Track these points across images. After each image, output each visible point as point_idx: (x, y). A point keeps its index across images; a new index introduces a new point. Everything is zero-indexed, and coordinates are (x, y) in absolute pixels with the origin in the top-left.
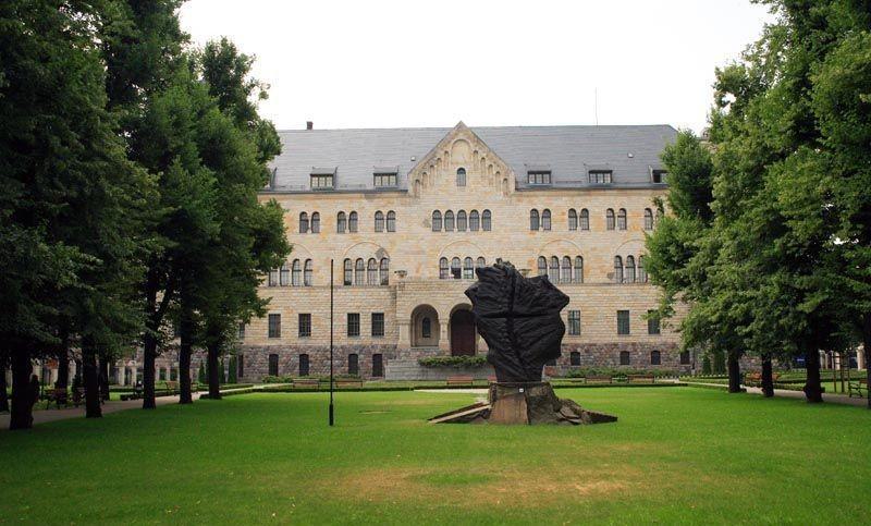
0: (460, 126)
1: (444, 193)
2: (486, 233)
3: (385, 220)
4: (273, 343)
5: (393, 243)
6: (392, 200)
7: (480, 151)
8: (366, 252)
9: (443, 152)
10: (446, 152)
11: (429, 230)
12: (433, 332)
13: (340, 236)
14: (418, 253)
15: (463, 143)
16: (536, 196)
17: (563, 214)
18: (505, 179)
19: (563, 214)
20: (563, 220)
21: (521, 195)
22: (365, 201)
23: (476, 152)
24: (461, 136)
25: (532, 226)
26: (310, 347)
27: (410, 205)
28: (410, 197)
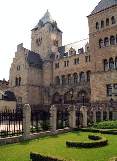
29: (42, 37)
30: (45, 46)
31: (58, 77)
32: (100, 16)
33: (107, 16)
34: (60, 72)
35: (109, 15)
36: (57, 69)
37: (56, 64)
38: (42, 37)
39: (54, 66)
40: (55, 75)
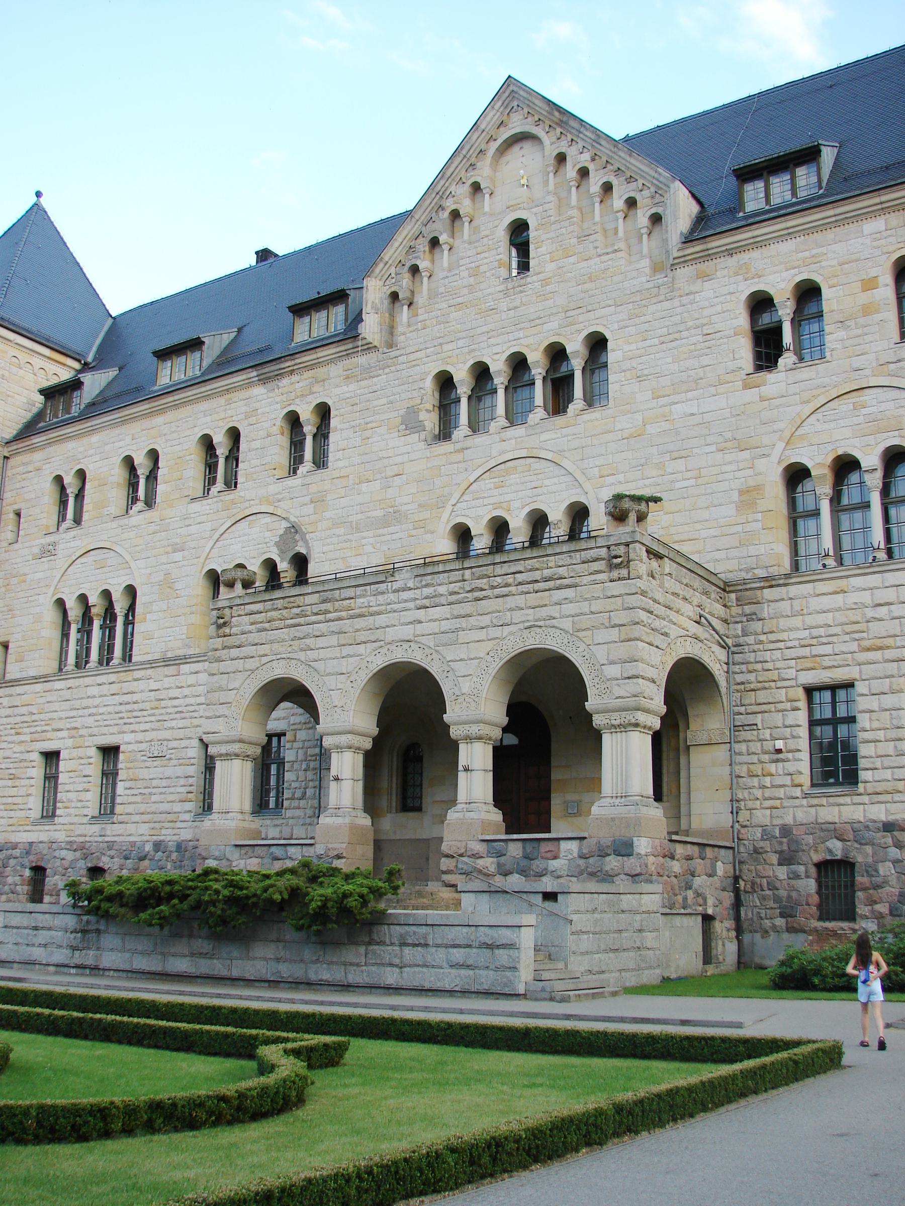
0: (512, 93)
1: (481, 314)
2: (595, 414)
3: (308, 438)
4: (40, 835)
5: (319, 501)
6: (321, 372)
7: (572, 153)
8: (252, 547)
9: (466, 189)
10: (476, 188)
11: (415, 444)
12: (431, 796)
13: (196, 507)
14: (385, 522)
15: (527, 145)
16: (757, 245)
17: (870, 284)
18: (656, 219)
19: (870, 284)
20: (867, 310)
21: (708, 256)
22: (259, 391)
23: (561, 158)
24: (517, 125)
25: (758, 356)
26: (110, 845)
27: (368, 373)
28: (369, 348)
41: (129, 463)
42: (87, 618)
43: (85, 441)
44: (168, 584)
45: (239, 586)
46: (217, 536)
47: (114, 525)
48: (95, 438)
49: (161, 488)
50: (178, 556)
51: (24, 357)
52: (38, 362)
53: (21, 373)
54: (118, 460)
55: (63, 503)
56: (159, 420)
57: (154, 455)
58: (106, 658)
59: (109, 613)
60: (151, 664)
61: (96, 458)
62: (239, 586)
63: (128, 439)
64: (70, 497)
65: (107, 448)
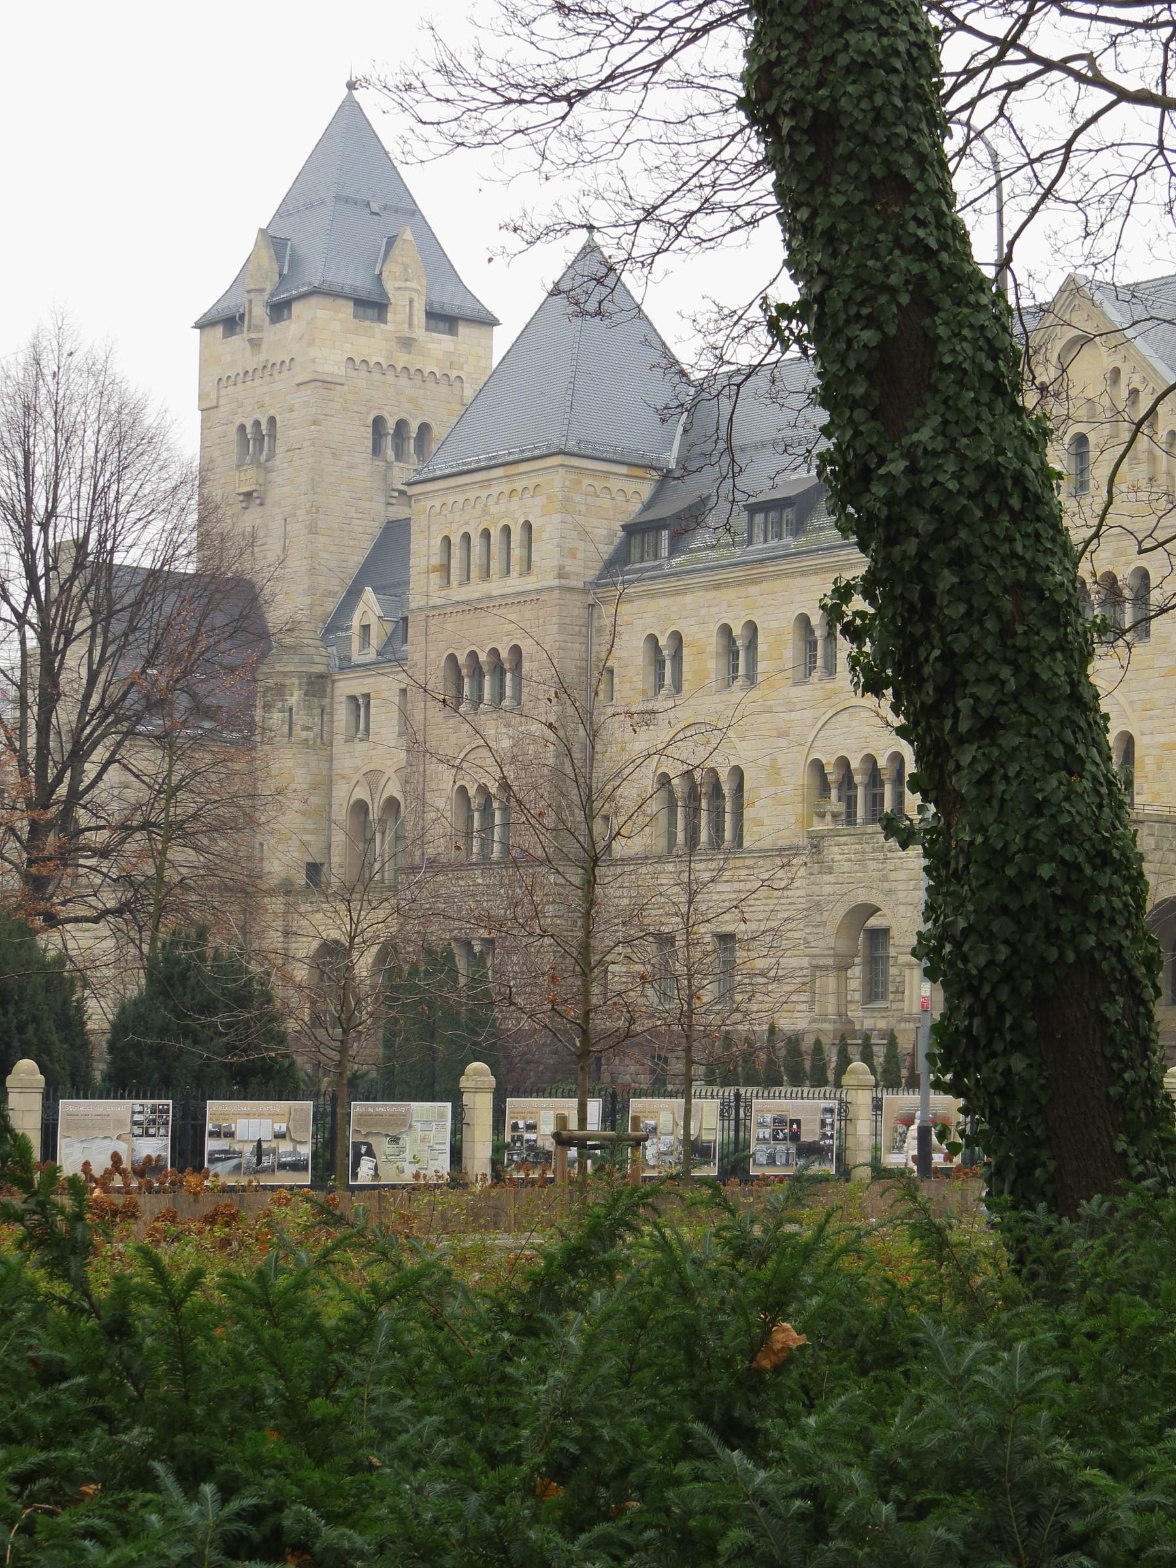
23: (1116, 372)
29: (272, 420)
30: (294, 515)
31: (360, 808)
32: (461, 499)
33: (485, 512)
34: (372, 777)
35: (494, 509)
36: (360, 747)
37: (353, 698)
38: (272, 420)
39: (342, 712)
40: (343, 796)
41: (726, 630)
42: (693, 796)
43: (678, 598)
44: (774, 771)
45: (828, 817)
46: (819, 725)
47: (717, 698)
48: (688, 599)
49: (762, 666)
50: (783, 742)
51: (598, 484)
52: (615, 484)
53: (599, 502)
54: (715, 628)
55: (660, 664)
56: (754, 590)
57: (752, 627)
58: (717, 840)
59: (716, 791)
60: (764, 853)
61: (693, 621)
62: (828, 817)
63: (724, 604)
64: (666, 657)
65: (703, 611)
